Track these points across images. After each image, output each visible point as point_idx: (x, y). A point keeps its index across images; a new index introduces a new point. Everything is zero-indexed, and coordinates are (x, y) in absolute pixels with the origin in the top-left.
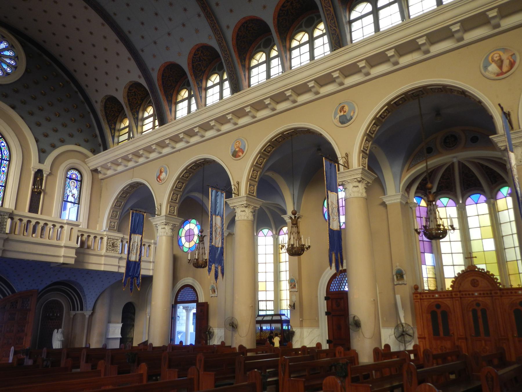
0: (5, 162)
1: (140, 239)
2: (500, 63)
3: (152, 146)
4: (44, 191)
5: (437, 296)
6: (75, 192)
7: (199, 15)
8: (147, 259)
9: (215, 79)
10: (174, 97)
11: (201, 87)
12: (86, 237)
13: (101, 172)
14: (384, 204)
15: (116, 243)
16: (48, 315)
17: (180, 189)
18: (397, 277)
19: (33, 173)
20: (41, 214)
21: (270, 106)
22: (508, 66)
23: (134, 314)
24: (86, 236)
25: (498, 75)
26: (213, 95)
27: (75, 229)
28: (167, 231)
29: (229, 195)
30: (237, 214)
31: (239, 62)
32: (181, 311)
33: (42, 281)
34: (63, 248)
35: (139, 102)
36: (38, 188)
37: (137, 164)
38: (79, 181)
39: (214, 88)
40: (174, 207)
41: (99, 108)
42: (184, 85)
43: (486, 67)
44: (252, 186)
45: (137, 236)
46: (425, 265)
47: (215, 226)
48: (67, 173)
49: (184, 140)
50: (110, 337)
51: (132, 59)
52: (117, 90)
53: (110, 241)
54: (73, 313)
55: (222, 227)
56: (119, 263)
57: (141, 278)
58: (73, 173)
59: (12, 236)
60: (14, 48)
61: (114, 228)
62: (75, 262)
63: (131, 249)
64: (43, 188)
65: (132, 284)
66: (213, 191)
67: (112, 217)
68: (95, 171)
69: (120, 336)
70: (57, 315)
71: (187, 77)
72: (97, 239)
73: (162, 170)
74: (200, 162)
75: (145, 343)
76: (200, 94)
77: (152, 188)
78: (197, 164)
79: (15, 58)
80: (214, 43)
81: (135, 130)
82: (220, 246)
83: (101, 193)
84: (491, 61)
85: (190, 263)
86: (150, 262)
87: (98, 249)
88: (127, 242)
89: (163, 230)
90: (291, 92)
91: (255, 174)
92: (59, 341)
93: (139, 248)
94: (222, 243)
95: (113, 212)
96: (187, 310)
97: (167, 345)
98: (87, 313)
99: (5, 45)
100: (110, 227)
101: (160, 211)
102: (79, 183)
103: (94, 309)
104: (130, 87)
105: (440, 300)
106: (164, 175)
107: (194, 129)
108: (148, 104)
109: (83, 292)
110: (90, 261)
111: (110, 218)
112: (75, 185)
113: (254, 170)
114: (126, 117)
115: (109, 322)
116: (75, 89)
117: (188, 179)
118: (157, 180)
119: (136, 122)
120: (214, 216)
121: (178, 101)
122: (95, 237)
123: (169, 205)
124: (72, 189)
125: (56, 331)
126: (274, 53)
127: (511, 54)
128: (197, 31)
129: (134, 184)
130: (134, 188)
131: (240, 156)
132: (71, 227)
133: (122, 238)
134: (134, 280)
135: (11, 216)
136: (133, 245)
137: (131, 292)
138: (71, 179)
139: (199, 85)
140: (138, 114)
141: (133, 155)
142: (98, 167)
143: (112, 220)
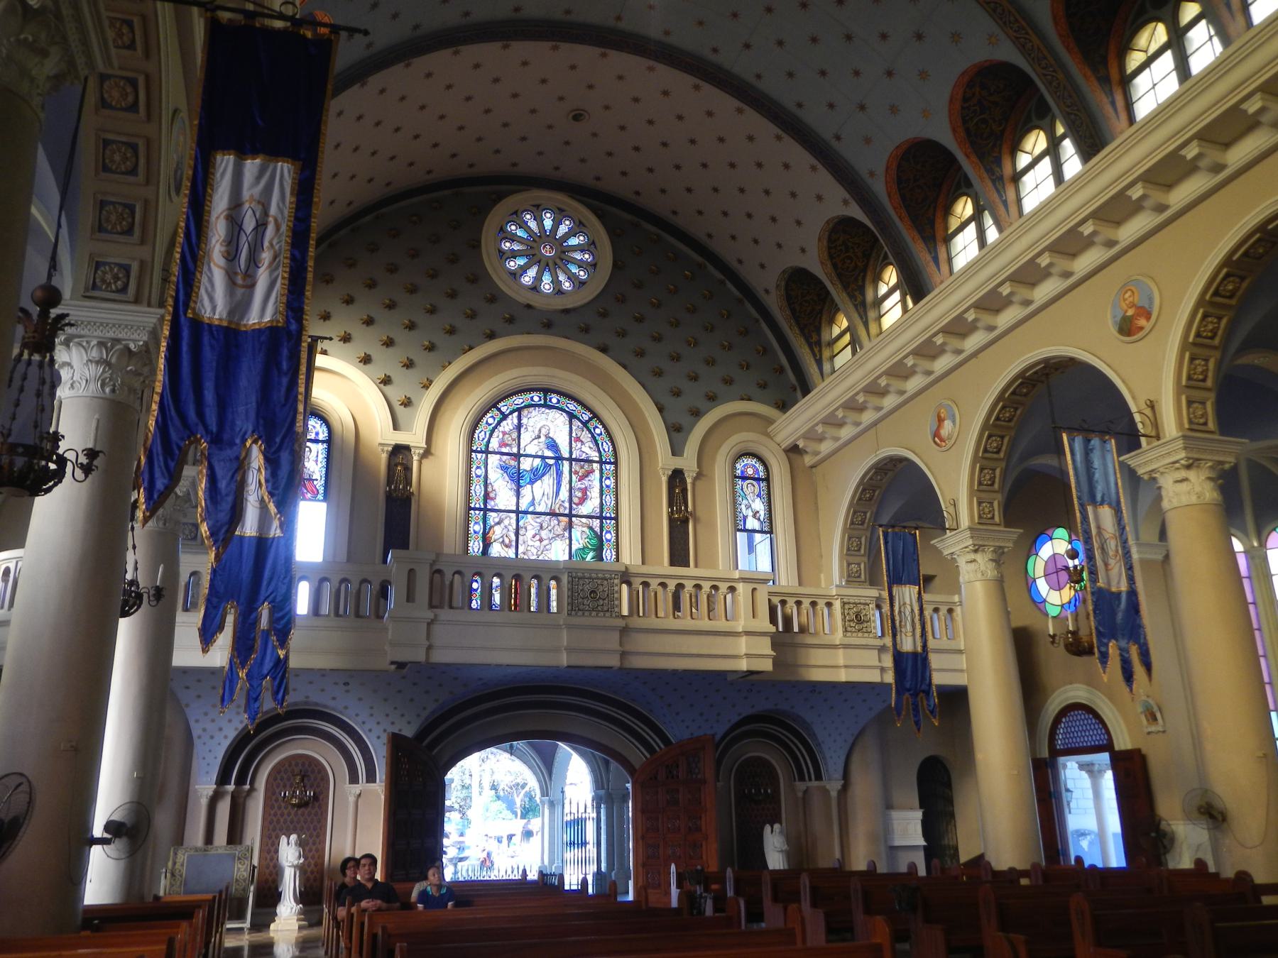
0: (608, 466)
3: (905, 361)
4: (693, 514)
6: (759, 505)
8: (952, 645)
9: (1036, 142)
11: (1001, 178)
13: (807, 450)
15: (864, 612)
16: (746, 791)
17: (998, 452)
19: (664, 479)
20: (696, 566)
21: (1203, 163)
23: (949, 785)
26: (1036, 187)
28: (983, 568)
29: (1130, 440)
30: (1164, 493)
31: (1089, 73)
32: (1072, 772)
33: (719, 714)
35: (859, 264)
36: (679, 511)
38: (763, 480)
40: (991, 504)
41: (774, 302)
42: (958, 187)
44: (1196, 405)
47: (1100, 533)
48: (734, 468)
49: (979, 325)
50: (897, 843)
51: (819, 166)
52: (803, 250)
54: (801, 786)
55: (1122, 534)
56: (880, 661)
57: (935, 694)
58: (746, 465)
59: (637, 622)
60: (584, 225)
61: (859, 577)
62: (774, 664)
63: (897, 623)
64: (690, 508)
65: (916, 709)
66: (1073, 440)
67: (850, 551)
68: (793, 451)
69: (922, 842)
70: (766, 791)
71: (960, 168)
72: (818, 607)
73: (942, 415)
74: (1036, 373)
75: (979, 861)
77: (926, 465)
78: (1028, 378)
79: (589, 247)
80: (1008, 53)
81: (862, 331)
82: (1124, 587)
83: (816, 498)
85: (1055, 645)
86: (960, 652)
89: (972, 566)
90: (1262, 99)
91: (1200, 369)
93: (917, 618)
94: (1131, 579)
95: (850, 538)
98: (834, 786)
100: (849, 576)
101: (956, 518)
102: (763, 484)
104: (830, 236)
106: (948, 425)
107: (1000, 290)
108: (883, 261)
109: (814, 736)
110: (813, 662)
111: (847, 555)
112: (757, 491)
113: (1192, 359)
114: (838, 310)
115: (889, 806)
116: (719, 276)
117: (1012, 424)
119: (862, 313)
120: (1090, 509)
121: (949, 232)
122: (814, 604)
123: (975, 499)
124: (751, 502)
125: (768, 828)
126: (1190, 11)
128: (956, 37)
129: (886, 464)
130: (886, 474)
131: (1141, 328)
134: (919, 699)
135: (626, 577)
136: (900, 612)
137: (919, 730)
138: (744, 478)
139: (993, 174)
140: (863, 294)
141: (867, 394)
142: (798, 439)
143: (852, 559)
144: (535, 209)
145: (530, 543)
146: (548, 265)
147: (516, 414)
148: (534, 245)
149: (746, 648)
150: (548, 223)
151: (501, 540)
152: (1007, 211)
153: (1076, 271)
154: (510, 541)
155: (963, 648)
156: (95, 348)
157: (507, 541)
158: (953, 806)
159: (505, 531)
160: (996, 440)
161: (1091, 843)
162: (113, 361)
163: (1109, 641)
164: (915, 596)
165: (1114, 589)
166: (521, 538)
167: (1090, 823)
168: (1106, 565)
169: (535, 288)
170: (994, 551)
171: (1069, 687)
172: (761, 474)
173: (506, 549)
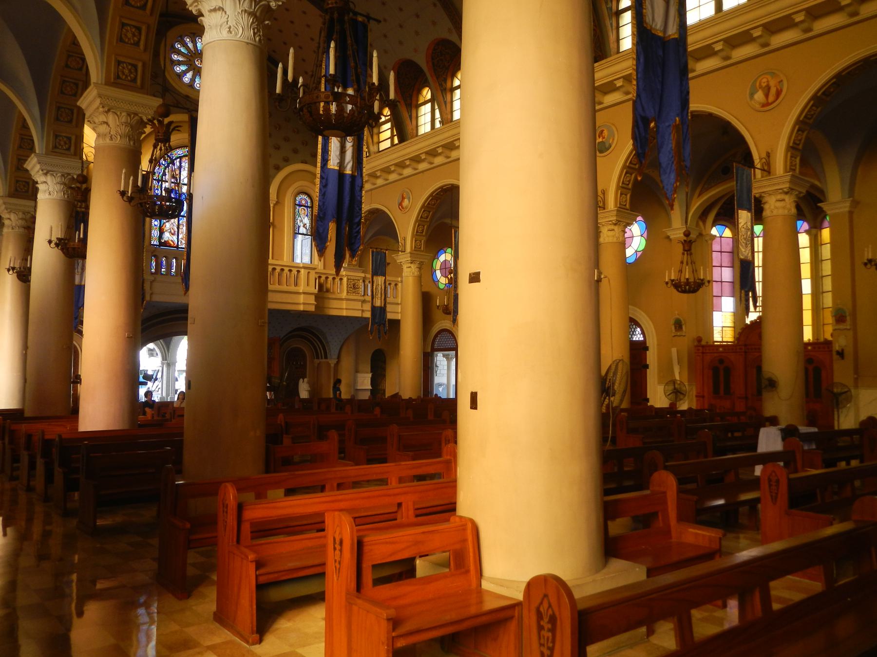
2: (767, 91)
4: (273, 224)
5: (721, 349)
10: (414, 99)
11: (445, 89)
12: (324, 279)
14: (668, 237)
15: (357, 284)
17: (427, 218)
18: (675, 328)
22: (774, 95)
23: (385, 362)
25: (764, 106)
27: (313, 273)
28: (413, 270)
37: (375, 186)
38: (309, 207)
40: (421, 241)
43: (752, 95)
45: (380, 278)
50: (359, 388)
54: (317, 361)
56: (362, 307)
58: (300, 199)
63: (375, 293)
70: (300, 363)
72: (336, 280)
75: (396, 396)
76: (444, 99)
84: (758, 88)
86: (398, 304)
87: (339, 292)
88: (370, 282)
89: (409, 269)
98: (333, 362)
101: (405, 246)
103: (339, 357)
115: (357, 371)
117: (434, 207)
118: (399, 207)
121: (419, 103)
125: (301, 380)
127: (778, 81)
132: (307, 271)
136: (376, 288)
138: (300, 205)
139: (442, 87)
144: (192, 35)
147: (178, 160)
151: (169, 231)
154: (174, 232)
155: (399, 302)
156: (59, 178)
157: (173, 231)
161: (443, 389)
162: (67, 182)
166: (180, 230)
171: (443, 321)
172: (309, 204)
173: (172, 236)
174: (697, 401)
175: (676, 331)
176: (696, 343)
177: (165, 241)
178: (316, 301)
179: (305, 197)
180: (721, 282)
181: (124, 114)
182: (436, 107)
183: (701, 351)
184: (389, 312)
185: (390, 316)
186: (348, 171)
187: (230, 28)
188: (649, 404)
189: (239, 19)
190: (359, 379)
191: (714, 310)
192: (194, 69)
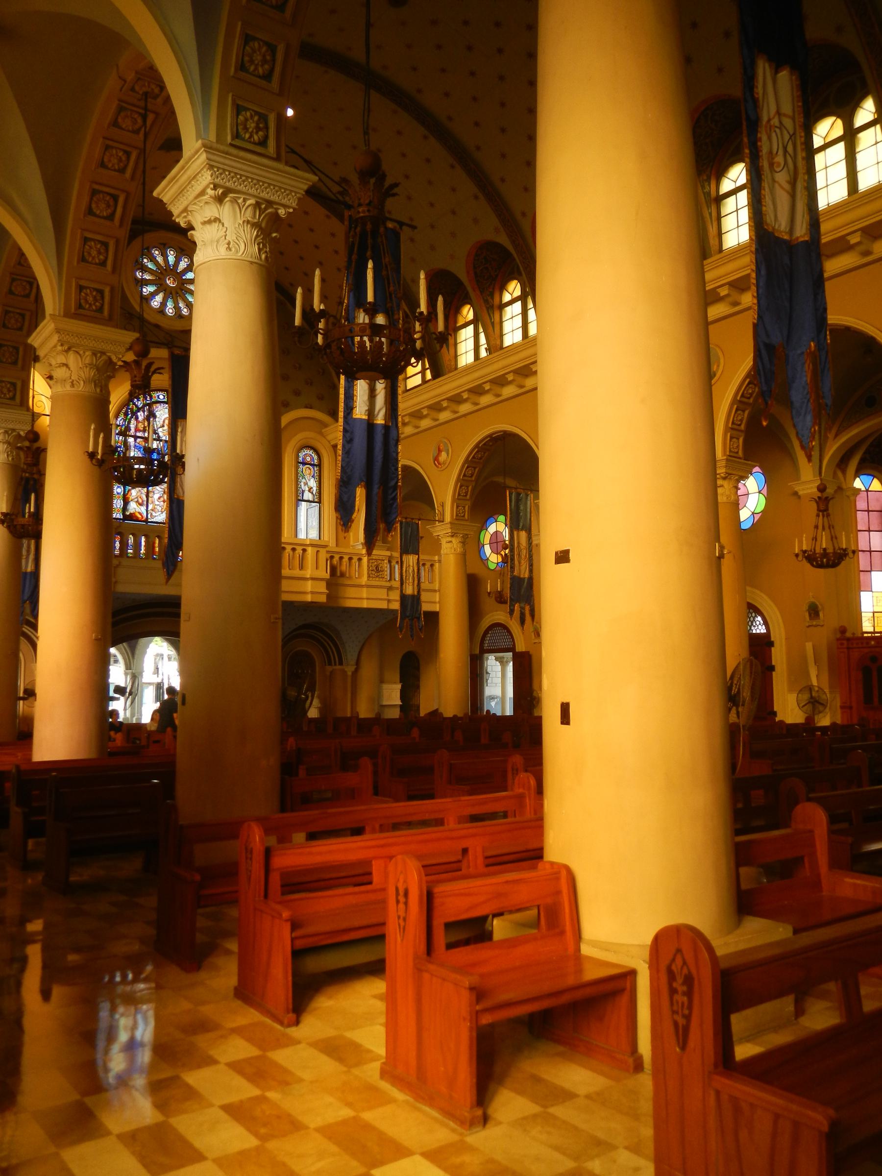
1: (416, 561)
5: (873, 643)
6: (313, 483)
7: (476, 197)
11: (492, 307)
12: (338, 559)
16: (295, 671)
18: (810, 615)
23: (418, 668)
24: (337, 557)
27: (323, 552)
28: (455, 546)
32: (492, 663)
34: (308, 580)
38: (316, 465)
39: (513, 305)
40: (464, 507)
45: (412, 557)
46: (872, 591)
47: (519, 546)
48: (298, 457)
50: (385, 703)
53: (372, 563)
54: (329, 668)
55: (530, 547)
56: (388, 596)
63: (404, 577)
69: (400, 703)
73: (441, 448)
75: (435, 713)
76: (491, 319)
82: (527, 576)
86: (435, 591)
87: (357, 576)
88: (397, 562)
89: (449, 545)
92: (315, 708)
94: (531, 571)
96: (500, 660)
97: (460, 715)
98: (349, 670)
99: (186, 263)
105: (877, 649)
106: (444, 454)
110: (347, 596)
115: (382, 681)
117: (481, 461)
118: (435, 464)
120: (515, 533)
121: (458, 325)
122: (350, 559)
123: (455, 504)
124: (307, 481)
128: (476, 221)
132: (316, 549)
133: (389, 556)
138: (304, 464)
144: (162, 246)
145: (157, 503)
146: (171, 294)
148: (160, 276)
149: (311, 588)
150: (171, 259)
151: (136, 500)
152: (494, 330)
153: (527, 386)
154: (143, 501)
157: (140, 501)
158: (419, 681)
159: (139, 494)
160: (471, 470)
162: (11, 441)
163: (516, 603)
164: (415, 562)
165: (522, 576)
166: (150, 499)
167: (498, 692)
168: (520, 563)
169: (161, 311)
170: (463, 537)
171: (495, 613)
172: (316, 461)
173: (140, 507)
174: (843, 713)
175: (810, 619)
176: (839, 635)
177: (130, 513)
178: (327, 589)
179: (310, 452)
180: (870, 551)
181: (88, 353)
182: (481, 330)
183: (845, 646)
184: (425, 602)
185: (425, 607)
186: (380, 420)
187: (229, 244)
188: (777, 719)
189: (240, 232)
190: (385, 691)
191: (862, 589)
192: (165, 290)
